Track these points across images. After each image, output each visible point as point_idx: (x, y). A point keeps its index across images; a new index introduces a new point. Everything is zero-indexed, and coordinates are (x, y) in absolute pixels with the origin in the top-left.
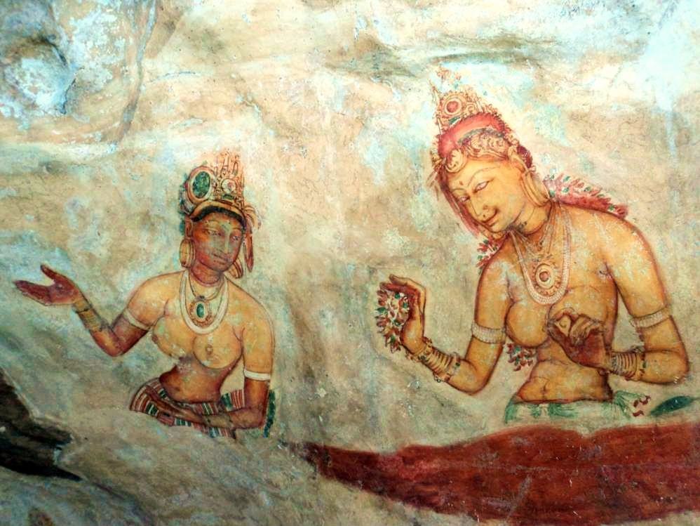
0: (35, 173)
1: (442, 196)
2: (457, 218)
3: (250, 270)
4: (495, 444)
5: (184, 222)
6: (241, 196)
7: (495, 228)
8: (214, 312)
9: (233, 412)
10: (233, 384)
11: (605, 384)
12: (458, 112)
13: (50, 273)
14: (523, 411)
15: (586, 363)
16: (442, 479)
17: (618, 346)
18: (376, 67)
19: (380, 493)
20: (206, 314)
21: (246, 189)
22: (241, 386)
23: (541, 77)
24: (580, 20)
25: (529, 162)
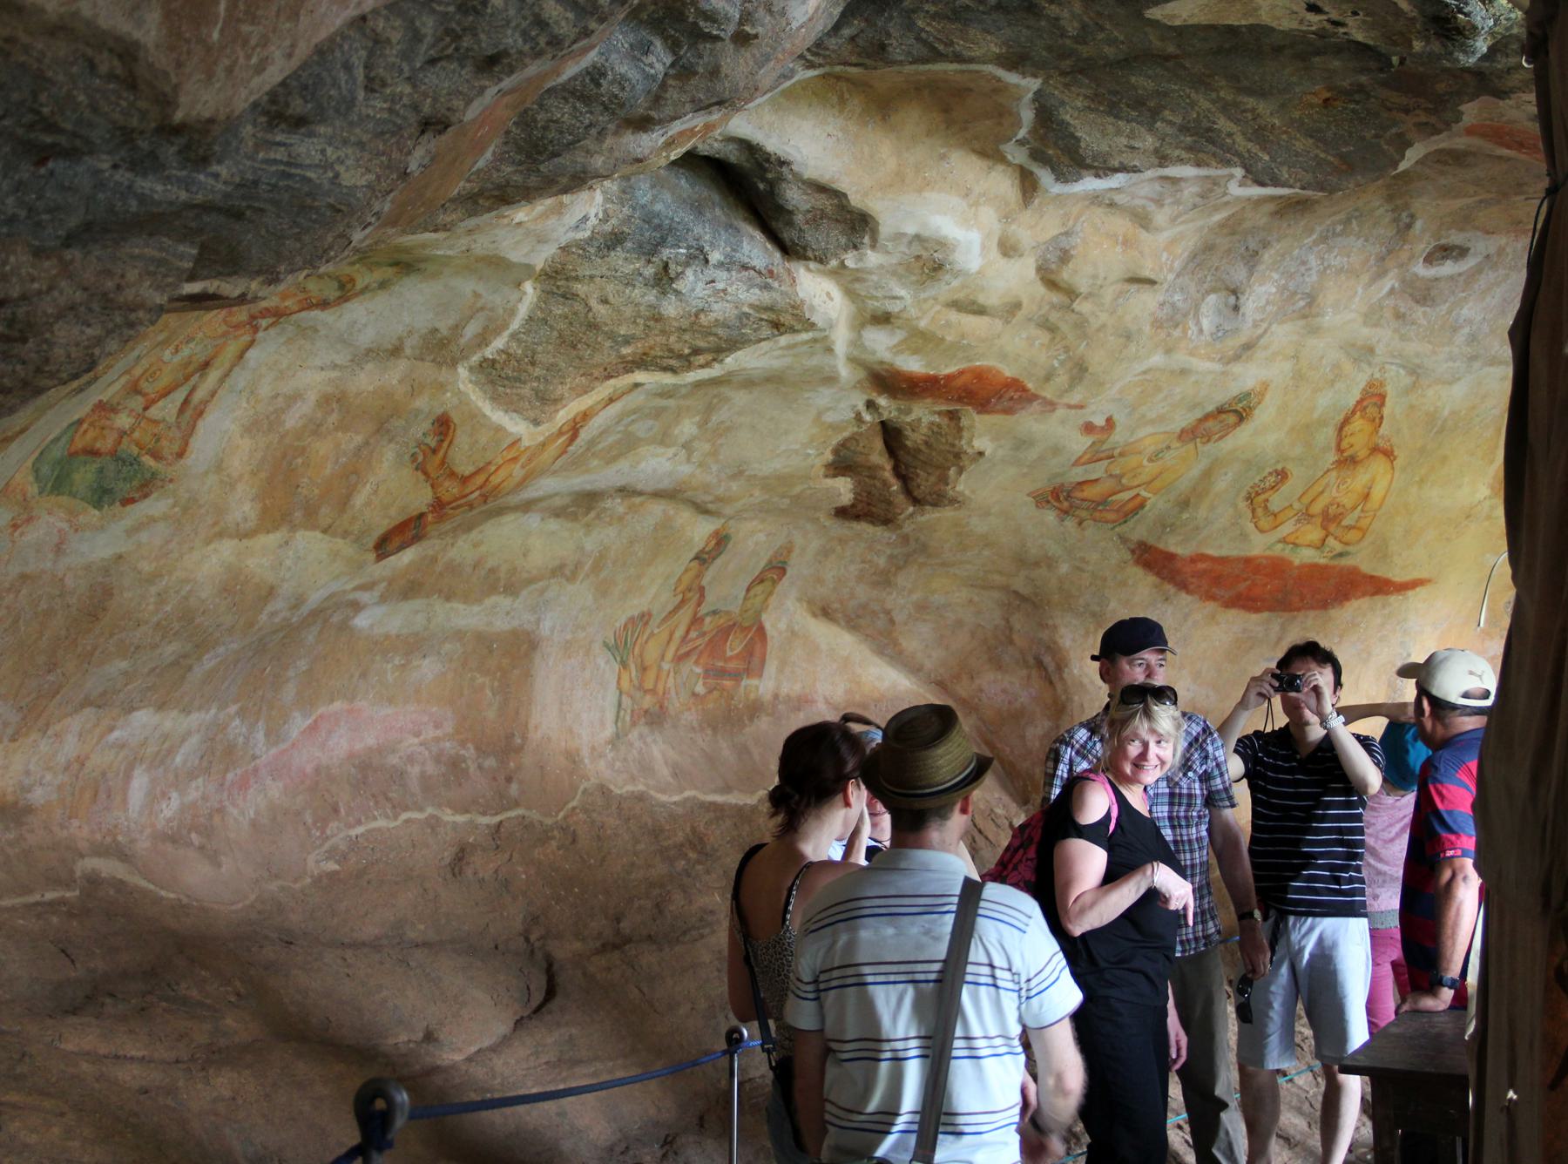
0: (1172, 372)
2: (1333, 445)
4: (1248, 561)
10: (1126, 496)
13: (1109, 420)
14: (1280, 546)
15: (1324, 528)
16: (1199, 575)
17: (1344, 523)
24: (1450, 364)
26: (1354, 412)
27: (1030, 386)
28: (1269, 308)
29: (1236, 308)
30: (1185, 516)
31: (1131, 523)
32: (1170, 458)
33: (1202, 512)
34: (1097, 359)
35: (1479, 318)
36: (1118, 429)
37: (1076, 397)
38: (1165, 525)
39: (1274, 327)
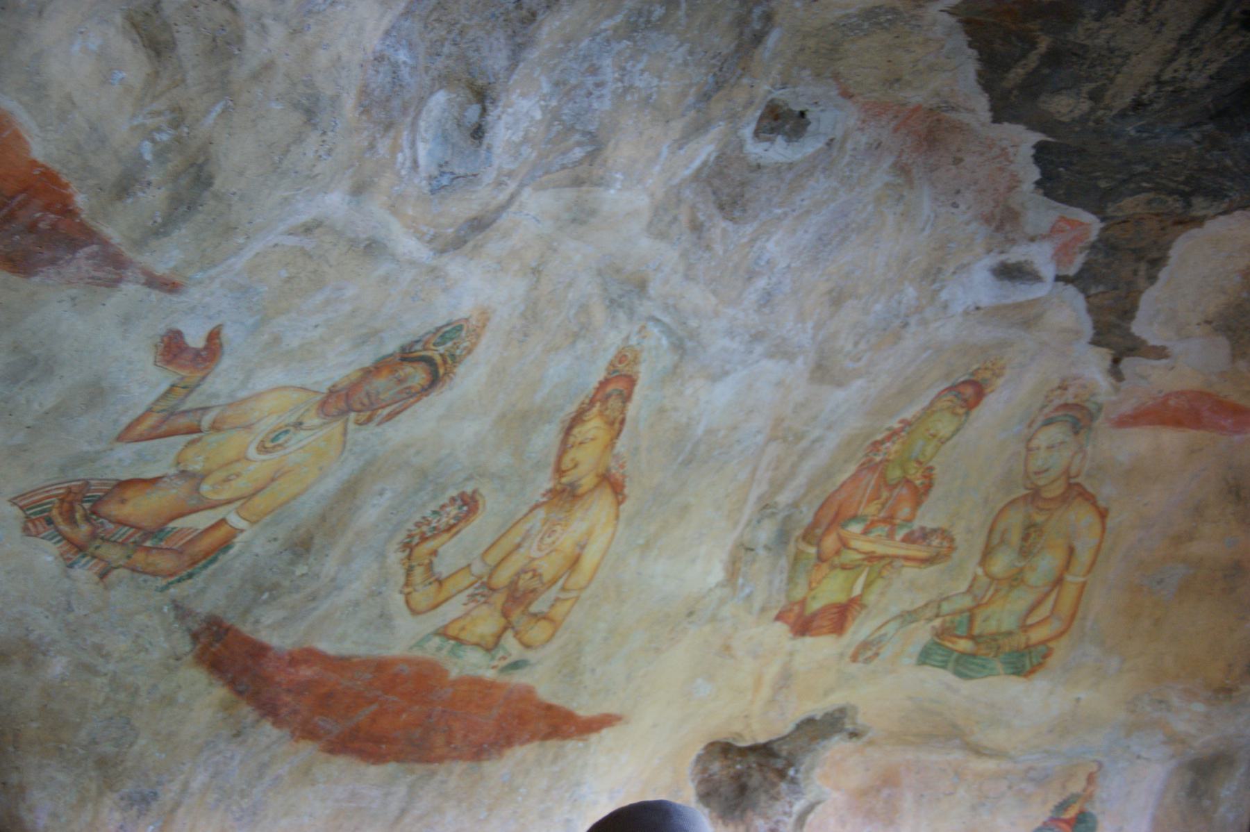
0: (353, 243)
1: (561, 436)
2: (552, 459)
3: (379, 424)
4: (380, 665)
5: (391, 355)
6: (460, 362)
7: (564, 480)
8: (292, 442)
9: (148, 549)
10: (201, 521)
11: (498, 637)
12: (620, 366)
13: (214, 337)
14: (437, 641)
15: (505, 614)
17: (534, 608)
18: (621, 296)
19: (240, 693)
20: (280, 441)
21: (470, 357)
22: (202, 527)
23: (676, 367)
24: (725, 342)
25: (620, 431)
26: (592, 402)
27: (81, 200)
28: (526, 150)
29: (478, 133)
30: (301, 569)
31: (199, 580)
32: (297, 447)
33: (330, 566)
34: (237, 155)
35: (783, 264)
36: (226, 363)
37: (166, 257)
38: (262, 588)
39: (526, 193)
